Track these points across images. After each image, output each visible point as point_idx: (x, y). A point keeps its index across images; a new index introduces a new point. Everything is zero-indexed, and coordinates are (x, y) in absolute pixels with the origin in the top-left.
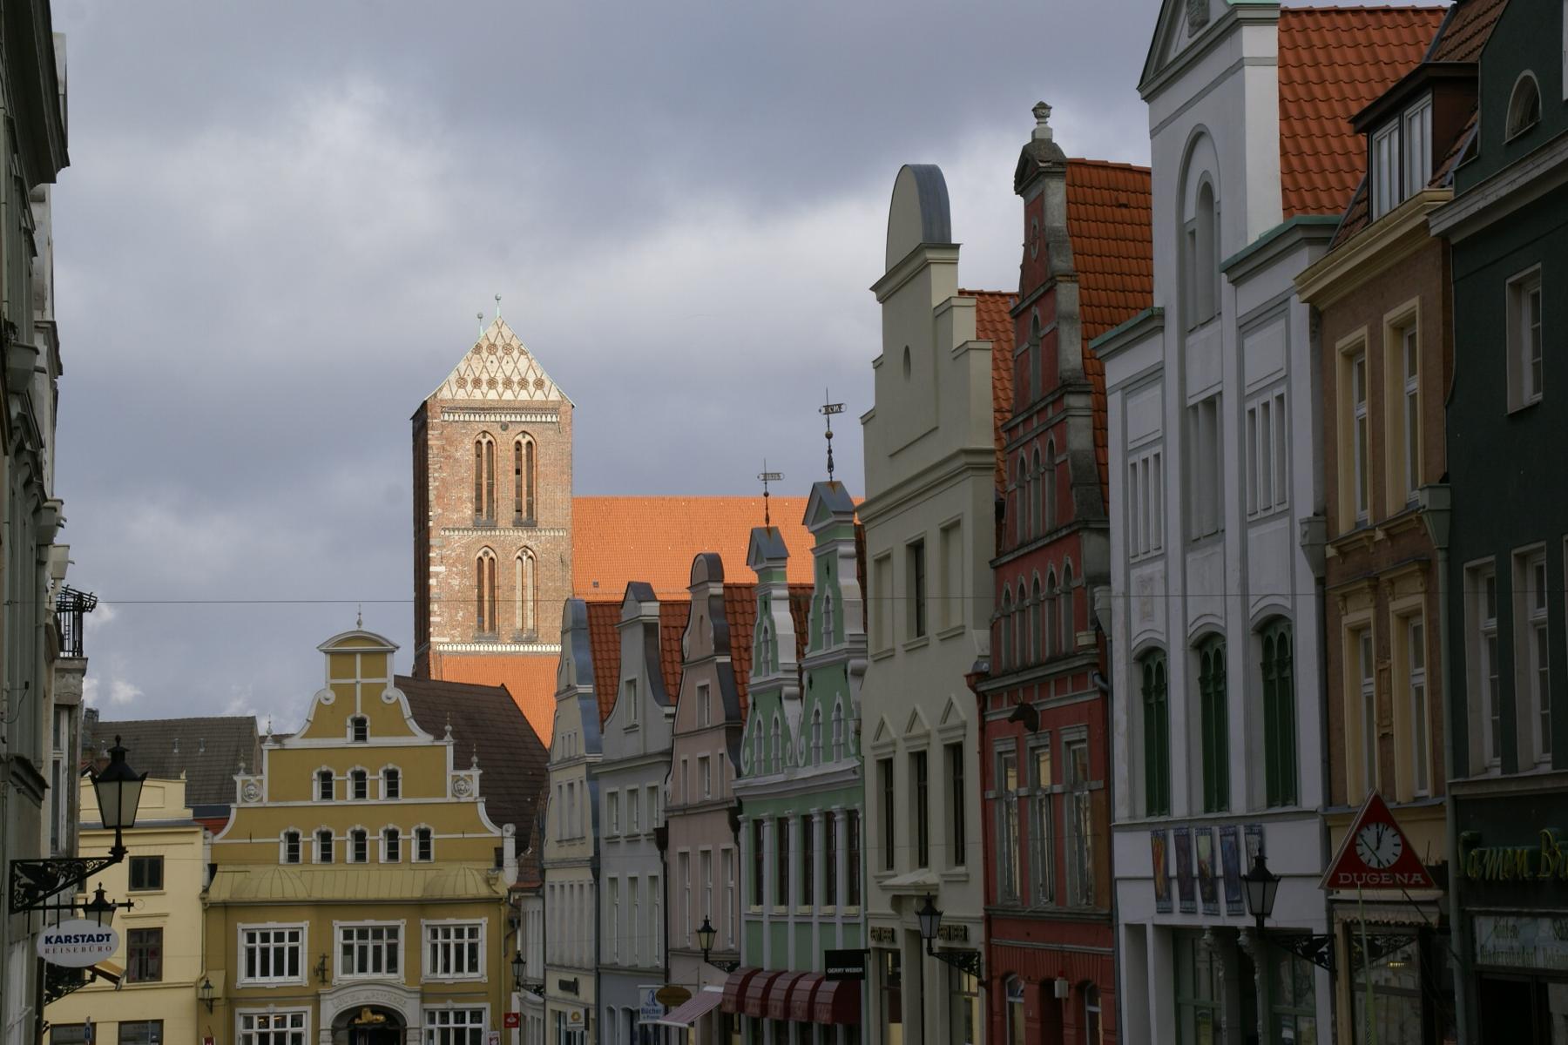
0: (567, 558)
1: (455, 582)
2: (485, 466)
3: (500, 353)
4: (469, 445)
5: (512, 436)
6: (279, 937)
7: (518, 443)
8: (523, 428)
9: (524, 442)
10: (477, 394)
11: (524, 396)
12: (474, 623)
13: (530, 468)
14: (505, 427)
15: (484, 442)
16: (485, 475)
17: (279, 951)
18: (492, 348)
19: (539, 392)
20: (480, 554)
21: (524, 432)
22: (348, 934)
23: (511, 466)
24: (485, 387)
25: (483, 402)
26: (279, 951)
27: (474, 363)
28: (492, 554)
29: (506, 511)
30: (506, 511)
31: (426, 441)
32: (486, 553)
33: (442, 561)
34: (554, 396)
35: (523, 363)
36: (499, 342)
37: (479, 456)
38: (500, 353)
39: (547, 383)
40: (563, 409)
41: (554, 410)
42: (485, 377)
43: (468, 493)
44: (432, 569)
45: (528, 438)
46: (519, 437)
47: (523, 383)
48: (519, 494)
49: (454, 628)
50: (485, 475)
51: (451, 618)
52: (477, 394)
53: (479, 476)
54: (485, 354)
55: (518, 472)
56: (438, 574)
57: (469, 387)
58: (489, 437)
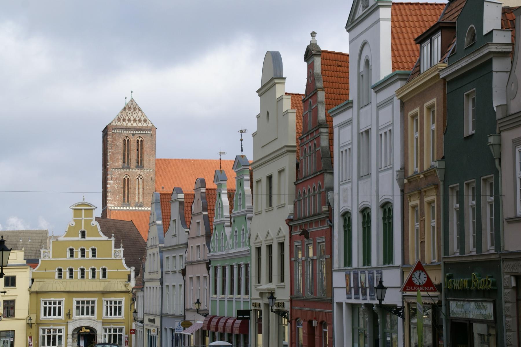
0: (154, 179)
1: (116, 186)
2: (126, 148)
3: (132, 110)
4: (121, 141)
5: (136, 138)
6: (55, 303)
7: (138, 140)
8: (140, 135)
9: (140, 140)
10: (124, 124)
11: (140, 125)
12: (122, 200)
13: (142, 149)
14: (133, 135)
15: (126, 140)
16: (126, 151)
17: (55, 308)
19: (145, 124)
20: (124, 177)
21: (140, 137)
22: (78, 303)
23: (135, 148)
24: (127, 122)
25: (127, 126)
26: (55, 308)
27: (123, 113)
28: (128, 177)
29: (133, 162)
30: (133, 162)
31: (107, 139)
32: (126, 177)
34: (150, 125)
36: (132, 107)
37: (124, 144)
38: (132, 110)
40: (153, 129)
41: (150, 130)
42: (127, 118)
43: (121, 157)
44: (108, 182)
45: (141, 139)
46: (138, 139)
48: (138, 157)
49: (115, 201)
50: (126, 151)
51: (115, 198)
52: (124, 124)
53: (124, 151)
54: (127, 111)
55: (138, 150)
56: (110, 183)
57: (122, 121)
58: (128, 138)
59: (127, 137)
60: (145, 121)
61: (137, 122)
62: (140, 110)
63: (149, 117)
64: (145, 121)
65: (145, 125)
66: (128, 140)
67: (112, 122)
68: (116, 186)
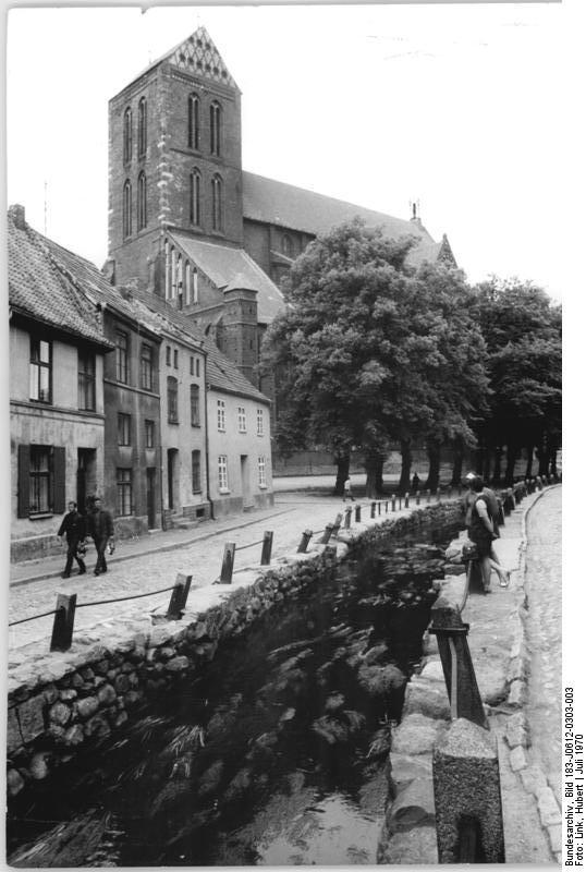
1: (178, 186)
2: (193, 115)
4: (186, 95)
7: (212, 108)
15: (194, 100)
21: (216, 102)
33: (171, 170)
36: (204, 42)
37: (190, 108)
38: (204, 48)
42: (195, 60)
47: (216, 70)
49: (178, 217)
50: (194, 123)
55: (212, 126)
59: (194, 94)
60: (225, 74)
62: (216, 51)
63: (231, 71)
65: (225, 81)
67: (170, 57)
68: (178, 186)
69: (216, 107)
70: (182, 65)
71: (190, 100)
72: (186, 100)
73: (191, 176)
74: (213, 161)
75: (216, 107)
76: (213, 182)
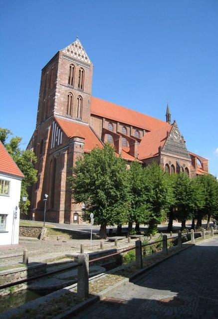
1: (62, 99)
18: (76, 46)
21: (82, 68)
29: (76, 85)
30: (76, 85)
35: (83, 52)
36: (78, 45)
37: (70, 70)
39: (88, 59)
42: (74, 52)
44: (56, 94)
47: (83, 57)
49: (61, 111)
55: (79, 77)
61: (81, 57)
64: (86, 58)
65: (86, 61)
66: (73, 68)
68: (62, 99)
69: (82, 70)
70: (68, 53)
71: (71, 67)
72: (69, 66)
73: (68, 96)
74: (78, 90)
75: (82, 70)
76: (78, 99)
